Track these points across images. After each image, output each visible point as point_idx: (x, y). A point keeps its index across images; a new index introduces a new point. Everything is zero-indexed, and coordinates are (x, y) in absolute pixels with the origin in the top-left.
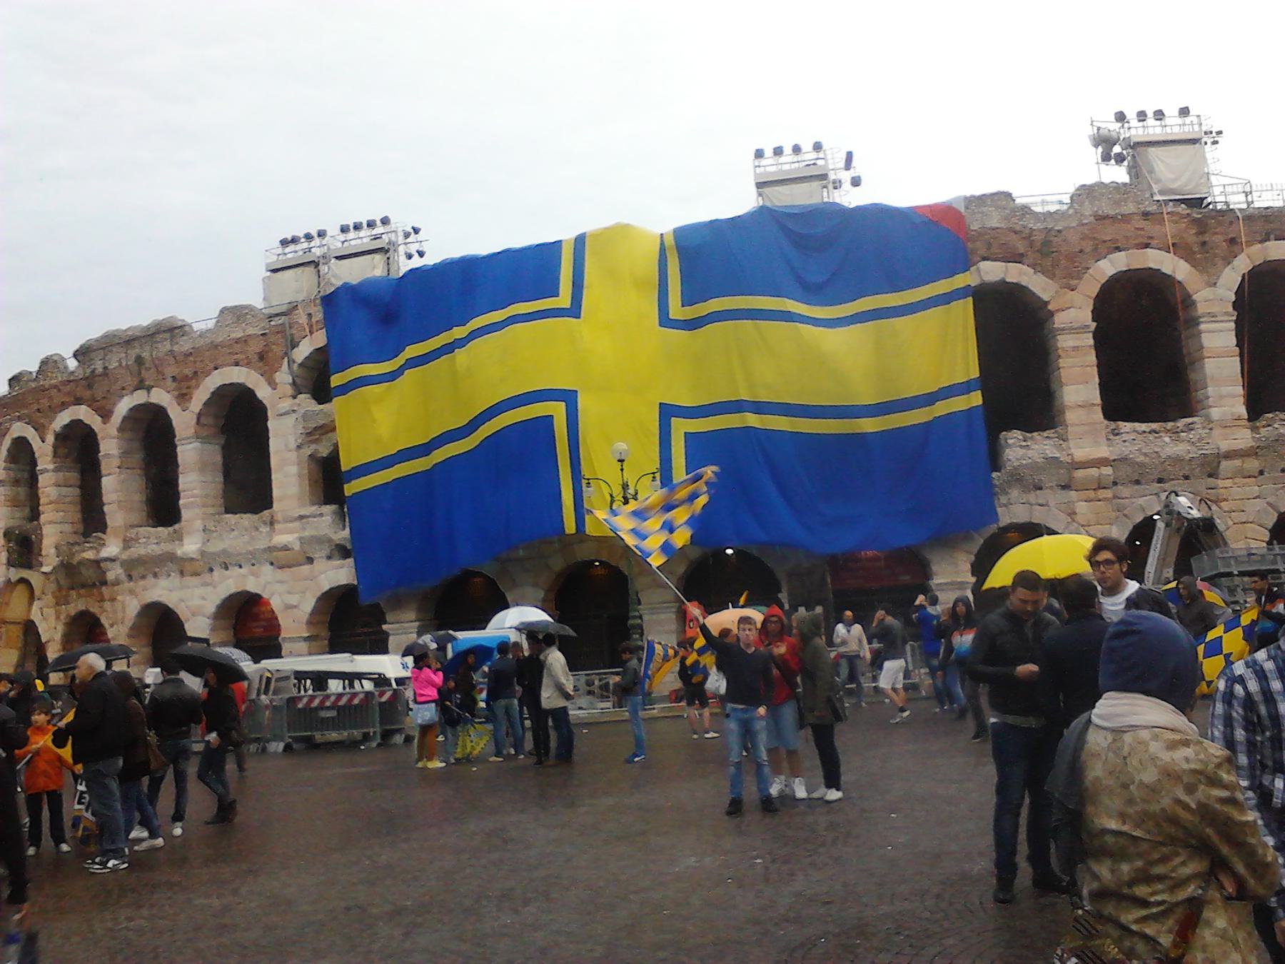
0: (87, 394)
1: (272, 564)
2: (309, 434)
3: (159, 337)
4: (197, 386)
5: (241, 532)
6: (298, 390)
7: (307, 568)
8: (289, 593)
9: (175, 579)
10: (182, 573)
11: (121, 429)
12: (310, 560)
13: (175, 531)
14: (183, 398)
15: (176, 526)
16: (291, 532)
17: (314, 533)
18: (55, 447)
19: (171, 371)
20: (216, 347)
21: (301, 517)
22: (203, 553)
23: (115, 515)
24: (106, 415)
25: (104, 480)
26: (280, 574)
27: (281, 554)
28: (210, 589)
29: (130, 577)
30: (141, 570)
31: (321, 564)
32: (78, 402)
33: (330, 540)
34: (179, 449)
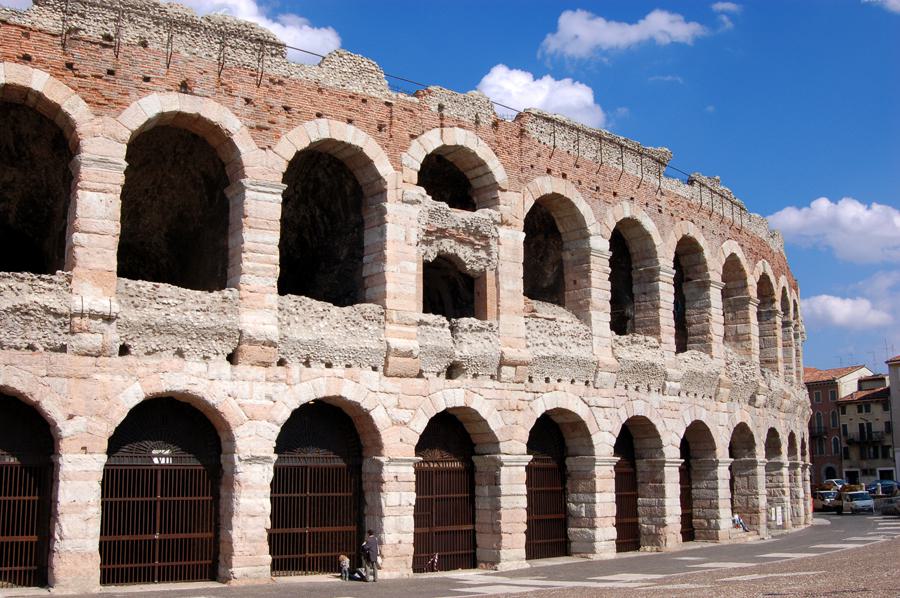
0: (58, 57)
1: (375, 369)
2: (428, 233)
3: (232, 41)
4: (290, 126)
5: (319, 321)
8: (398, 406)
10: (232, 358)
12: (420, 375)
20: (320, 90)
21: (421, 323)
22: (284, 338)
26: (390, 384)
28: (282, 387)
29: (124, 350)
30: (153, 342)
32: (26, 58)
34: (248, 193)
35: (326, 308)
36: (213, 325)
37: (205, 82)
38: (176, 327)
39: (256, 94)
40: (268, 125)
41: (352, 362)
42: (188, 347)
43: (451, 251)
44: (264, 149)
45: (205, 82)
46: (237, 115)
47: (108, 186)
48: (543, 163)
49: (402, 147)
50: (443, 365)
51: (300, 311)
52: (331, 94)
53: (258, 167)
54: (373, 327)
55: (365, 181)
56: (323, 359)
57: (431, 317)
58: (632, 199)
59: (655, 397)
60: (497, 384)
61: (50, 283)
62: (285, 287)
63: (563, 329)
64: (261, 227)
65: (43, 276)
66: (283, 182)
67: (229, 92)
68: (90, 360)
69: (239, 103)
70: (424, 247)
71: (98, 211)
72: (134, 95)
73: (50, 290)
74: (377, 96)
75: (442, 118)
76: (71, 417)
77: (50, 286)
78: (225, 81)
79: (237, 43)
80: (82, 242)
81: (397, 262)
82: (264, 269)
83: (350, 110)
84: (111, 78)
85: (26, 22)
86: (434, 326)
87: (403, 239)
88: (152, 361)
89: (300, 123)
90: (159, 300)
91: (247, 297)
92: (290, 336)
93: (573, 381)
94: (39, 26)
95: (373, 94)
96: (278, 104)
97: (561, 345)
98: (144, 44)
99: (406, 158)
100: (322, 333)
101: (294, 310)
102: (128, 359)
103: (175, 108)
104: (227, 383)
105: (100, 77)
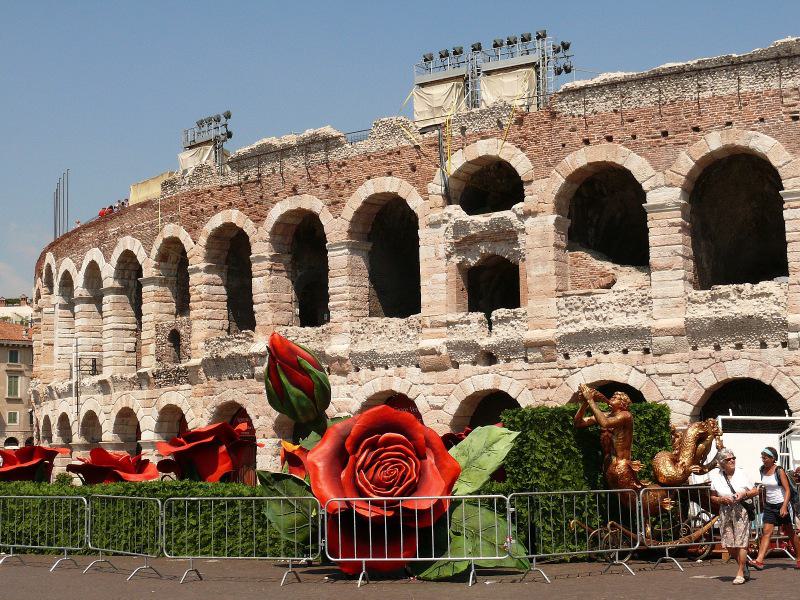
5: (390, 335)
6: (449, 199)
7: (452, 371)
8: (433, 394)
11: (273, 233)
12: (456, 365)
13: (323, 331)
14: (335, 205)
15: (324, 327)
17: (461, 338)
18: (207, 247)
19: (323, 179)
21: (448, 324)
23: (263, 313)
24: (259, 220)
25: (255, 281)
31: (466, 368)
33: (477, 346)
48: (577, 137)
51: (366, 330)
54: (411, 333)
58: (729, 124)
59: (774, 353)
60: (526, 366)
63: (599, 302)
69: (321, 190)
76: (258, 417)
81: (429, 276)
82: (341, 305)
93: (625, 352)
97: (597, 318)
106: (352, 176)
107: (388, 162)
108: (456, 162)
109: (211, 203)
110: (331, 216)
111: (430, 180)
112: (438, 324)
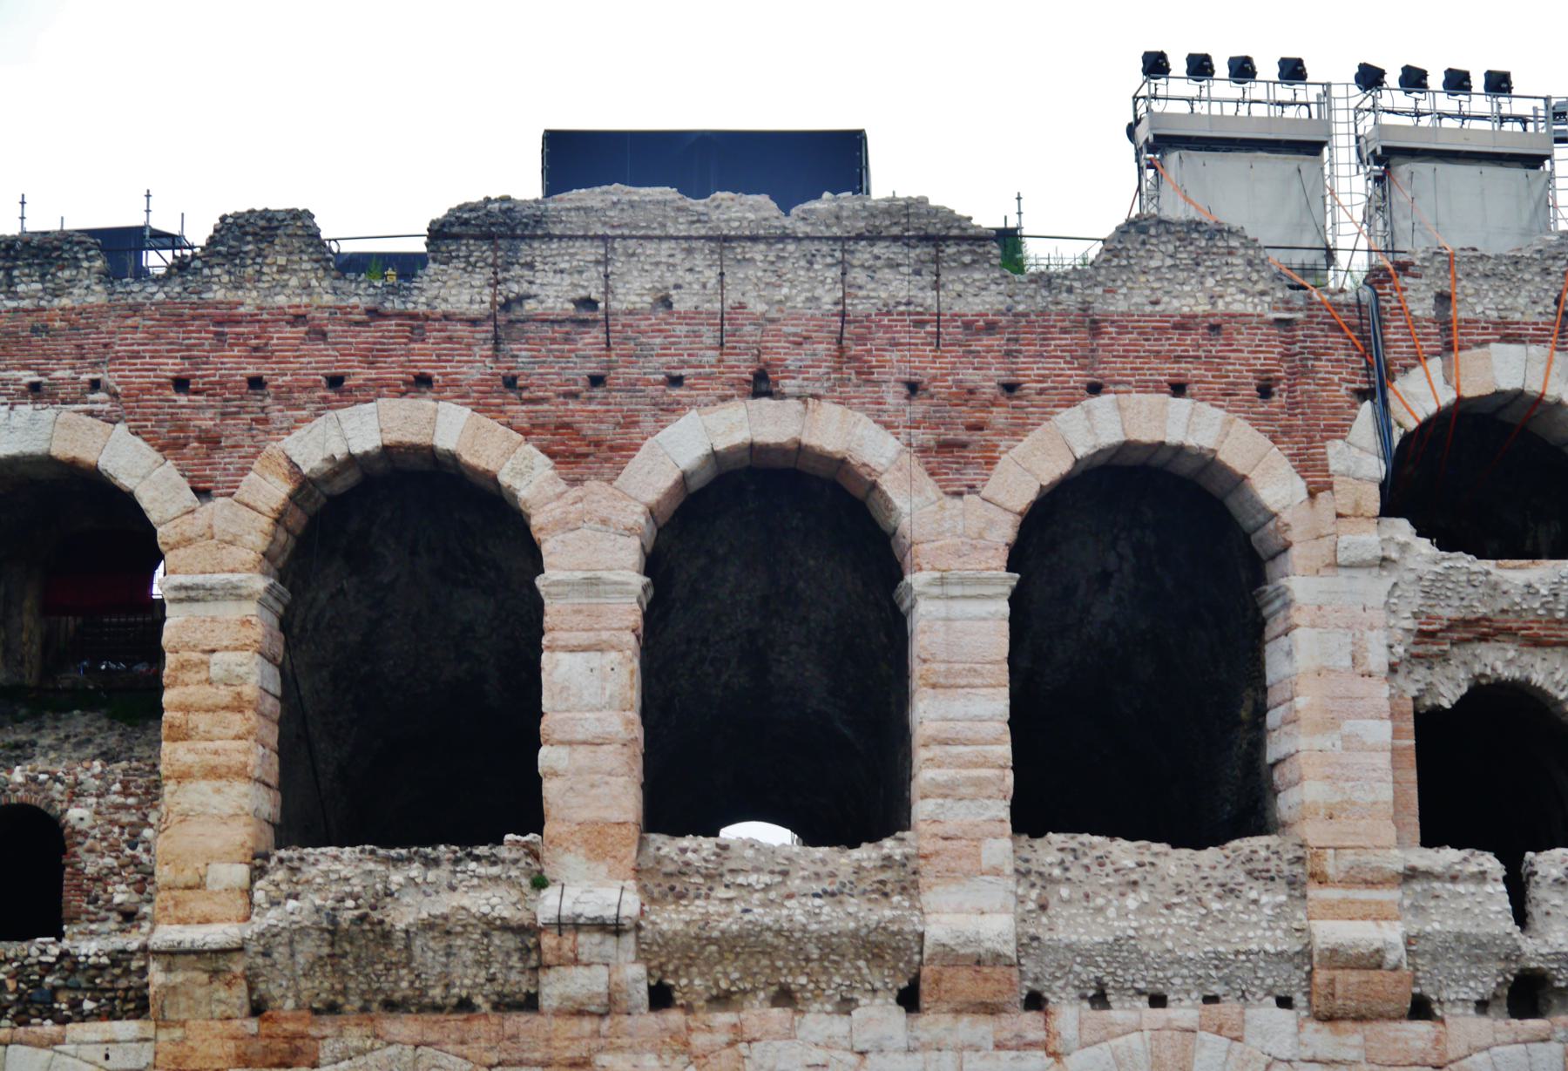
0: (477, 367)
1: (1285, 1002)
3: (863, 253)
4: (1018, 429)
7: (1422, 1027)
9: (880, 1017)
10: (909, 999)
12: (1421, 1009)
14: (954, 456)
15: (888, 845)
16: (1379, 914)
17: (1468, 927)
19: (895, 365)
21: (1411, 875)
22: (1028, 943)
27: (1354, 977)
29: (660, 997)
32: (422, 383)
35: (1147, 859)
36: (852, 925)
37: (804, 365)
38: (769, 936)
39: (926, 365)
40: (964, 436)
41: (1216, 989)
42: (803, 980)
43: (1508, 673)
44: (959, 494)
45: (804, 365)
46: (888, 426)
47: (605, 635)
49: (1329, 428)
50: (1488, 981)
52: (1123, 330)
53: (948, 540)
55: (1251, 523)
56: (1141, 985)
57: (1446, 857)
61: (494, 863)
62: (1032, 814)
64: (963, 682)
65: (481, 850)
66: (1009, 569)
67: (865, 374)
68: (587, 1025)
69: (893, 396)
70: (1421, 672)
71: (590, 697)
72: (648, 423)
73: (497, 878)
74: (1250, 310)
75: (1446, 326)
77: (495, 870)
78: (855, 350)
79: (878, 258)
80: (561, 765)
82: (978, 783)
83: (1178, 359)
84: (598, 393)
85: (418, 303)
86: (1454, 879)
87: (1347, 662)
88: (723, 1018)
89: (1046, 416)
90: (728, 878)
91: (937, 853)
92: (1045, 936)
94: (443, 307)
95: (1237, 308)
96: (987, 378)
98: (666, 302)
99: (1337, 454)
100: (1126, 927)
101: (1057, 872)
102: (674, 1017)
103: (740, 437)
104: (900, 1057)
105: (575, 395)
106: (1031, 371)
107: (1185, 355)
108: (1421, 395)
109: (315, 362)
110: (930, 488)
111: (1339, 430)
112: (1377, 877)
